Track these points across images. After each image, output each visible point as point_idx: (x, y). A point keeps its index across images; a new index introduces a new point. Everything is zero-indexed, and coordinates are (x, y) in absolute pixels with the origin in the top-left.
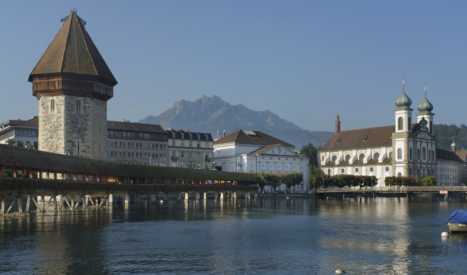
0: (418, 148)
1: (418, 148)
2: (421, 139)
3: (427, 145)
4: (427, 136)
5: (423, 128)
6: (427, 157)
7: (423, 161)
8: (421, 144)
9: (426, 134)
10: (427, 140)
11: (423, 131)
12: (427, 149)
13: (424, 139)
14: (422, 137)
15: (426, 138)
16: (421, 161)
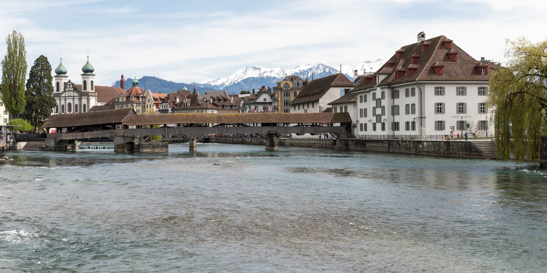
0: (61, 104)
1: (61, 104)
2: (66, 97)
3: (74, 100)
4: (73, 93)
5: (70, 88)
6: (74, 110)
7: (67, 113)
8: (65, 101)
9: (72, 92)
10: (74, 96)
11: (67, 91)
12: (74, 104)
13: (70, 96)
14: (67, 95)
15: (72, 95)
16: (66, 113)
